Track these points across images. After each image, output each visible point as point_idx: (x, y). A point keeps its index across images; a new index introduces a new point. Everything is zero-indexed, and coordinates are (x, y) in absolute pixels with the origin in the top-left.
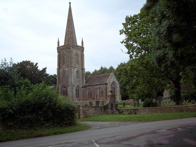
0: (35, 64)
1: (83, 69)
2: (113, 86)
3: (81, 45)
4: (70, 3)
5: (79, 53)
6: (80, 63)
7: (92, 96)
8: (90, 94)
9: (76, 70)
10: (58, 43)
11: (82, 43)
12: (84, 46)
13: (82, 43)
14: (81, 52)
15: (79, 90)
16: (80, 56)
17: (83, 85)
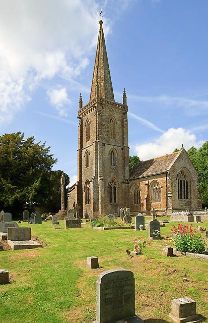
0: (25, 139)
2: (182, 178)
5: (117, 116)
6: (119, 137)
10: (81, 102)
15: (115, 188)
16: (119, 123)
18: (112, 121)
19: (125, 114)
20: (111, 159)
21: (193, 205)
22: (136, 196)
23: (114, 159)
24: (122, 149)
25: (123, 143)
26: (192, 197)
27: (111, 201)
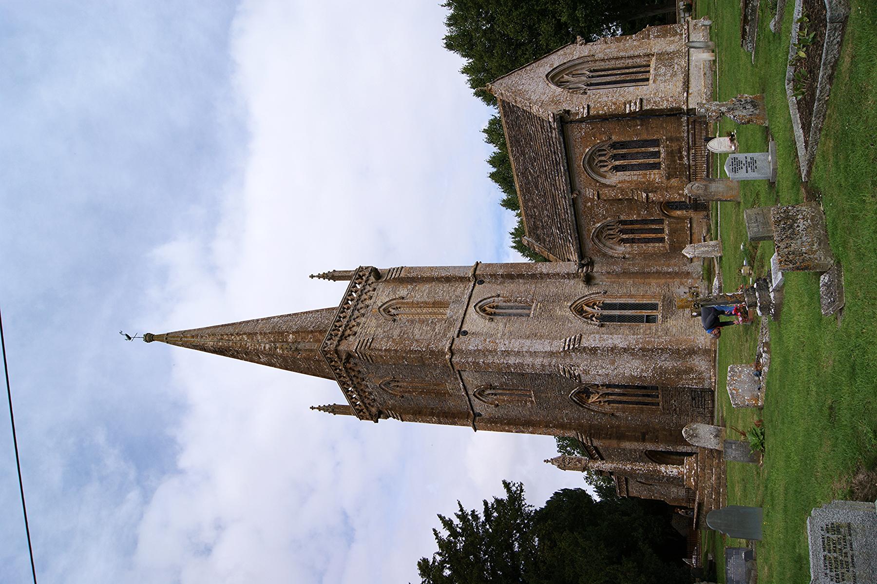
1: (474, 275)
3: (345, 284)
4: (149, 338)
5: (383, 295)
6: (442, 292)
7: (644, 222)
8: (632, 231)
9: (475, 322)
10: (334, 409)
11: (333, 276)
12: (353, 267)
13: (333, 276)
14: (381, 286)
15: (606, 306)
16: (403, 291)
17: (576, 276)
18: (393, 311)
19: (376, 273)
20: (510, 315)
21: (672, 48)
22: (637, 236)
23: (512, 308)
24: (481, 282)
25: (463, 279)
26: (641, 52)
27: (650, 320)
